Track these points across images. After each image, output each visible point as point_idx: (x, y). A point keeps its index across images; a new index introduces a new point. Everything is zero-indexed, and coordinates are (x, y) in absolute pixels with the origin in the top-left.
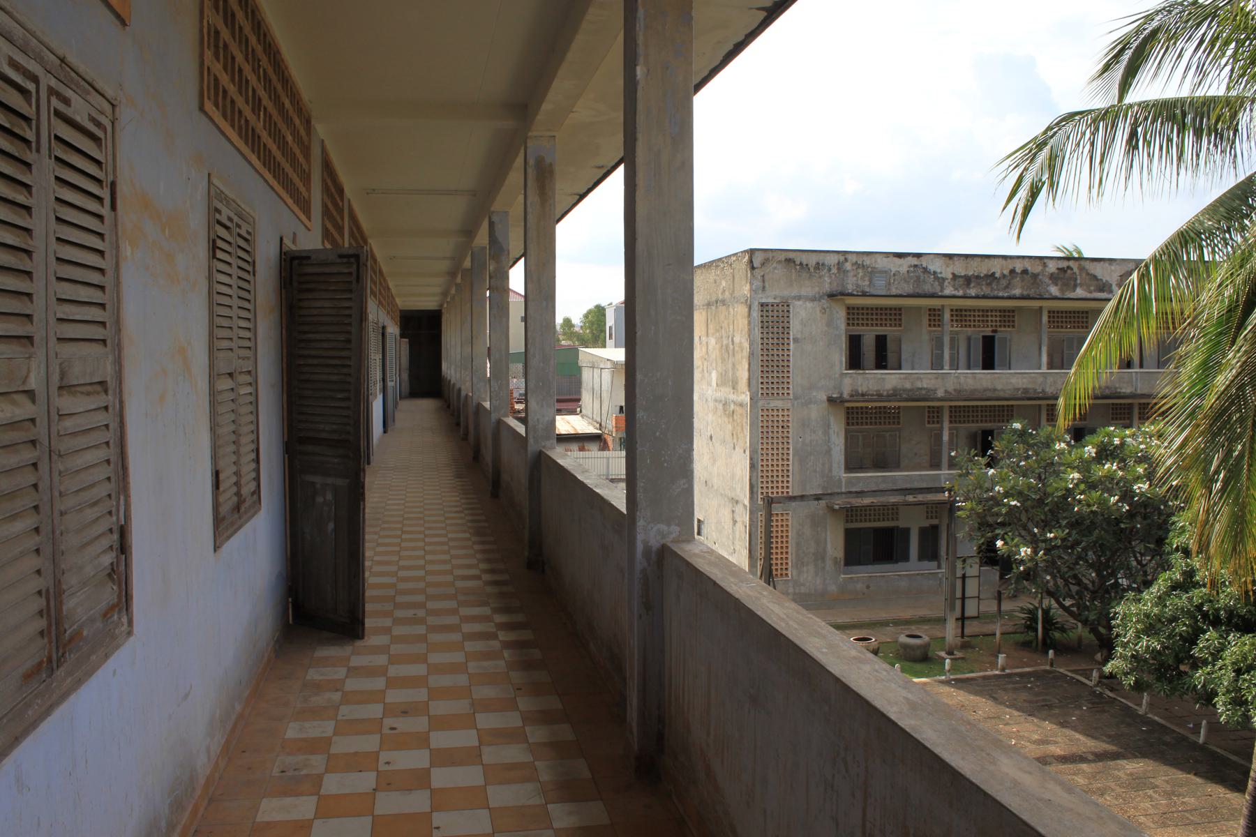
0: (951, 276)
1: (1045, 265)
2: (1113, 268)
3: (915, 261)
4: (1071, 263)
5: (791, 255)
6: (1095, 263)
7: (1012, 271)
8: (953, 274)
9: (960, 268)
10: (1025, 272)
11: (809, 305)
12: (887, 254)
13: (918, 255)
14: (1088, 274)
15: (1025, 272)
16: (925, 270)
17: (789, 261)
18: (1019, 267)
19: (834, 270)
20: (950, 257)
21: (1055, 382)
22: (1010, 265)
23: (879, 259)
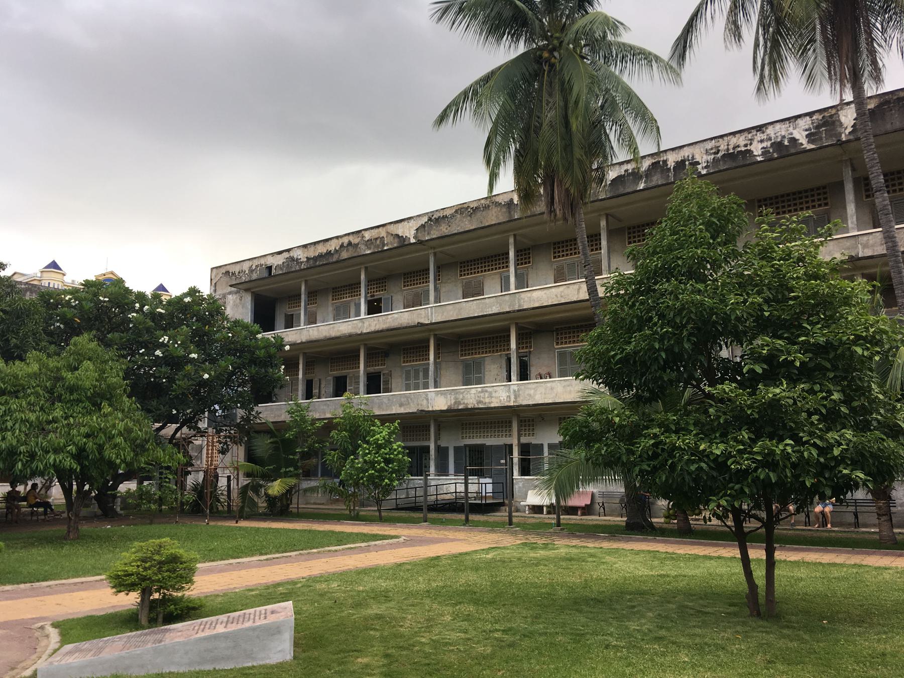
0: (305, 260)
1: (363, 237)
2: (411, 224)
3: (286, 255)
4: (380, 229)
5: (228, 268)
6: (397, 225)
7: (342, 246)
8: (307, 258)
9: (312, 253)
10: (350, 244)
11: (235, 296)
12: (272, 254)
13: (288, 250)
14: (392, 235)
15: (350, 244)
16: (292, 259)
17: (227, 273)
18: (346, 240)
19: (247, 272)
20: (305, 246)
21: (370, 325)
22: (341, 241)
23: (270, 258)
